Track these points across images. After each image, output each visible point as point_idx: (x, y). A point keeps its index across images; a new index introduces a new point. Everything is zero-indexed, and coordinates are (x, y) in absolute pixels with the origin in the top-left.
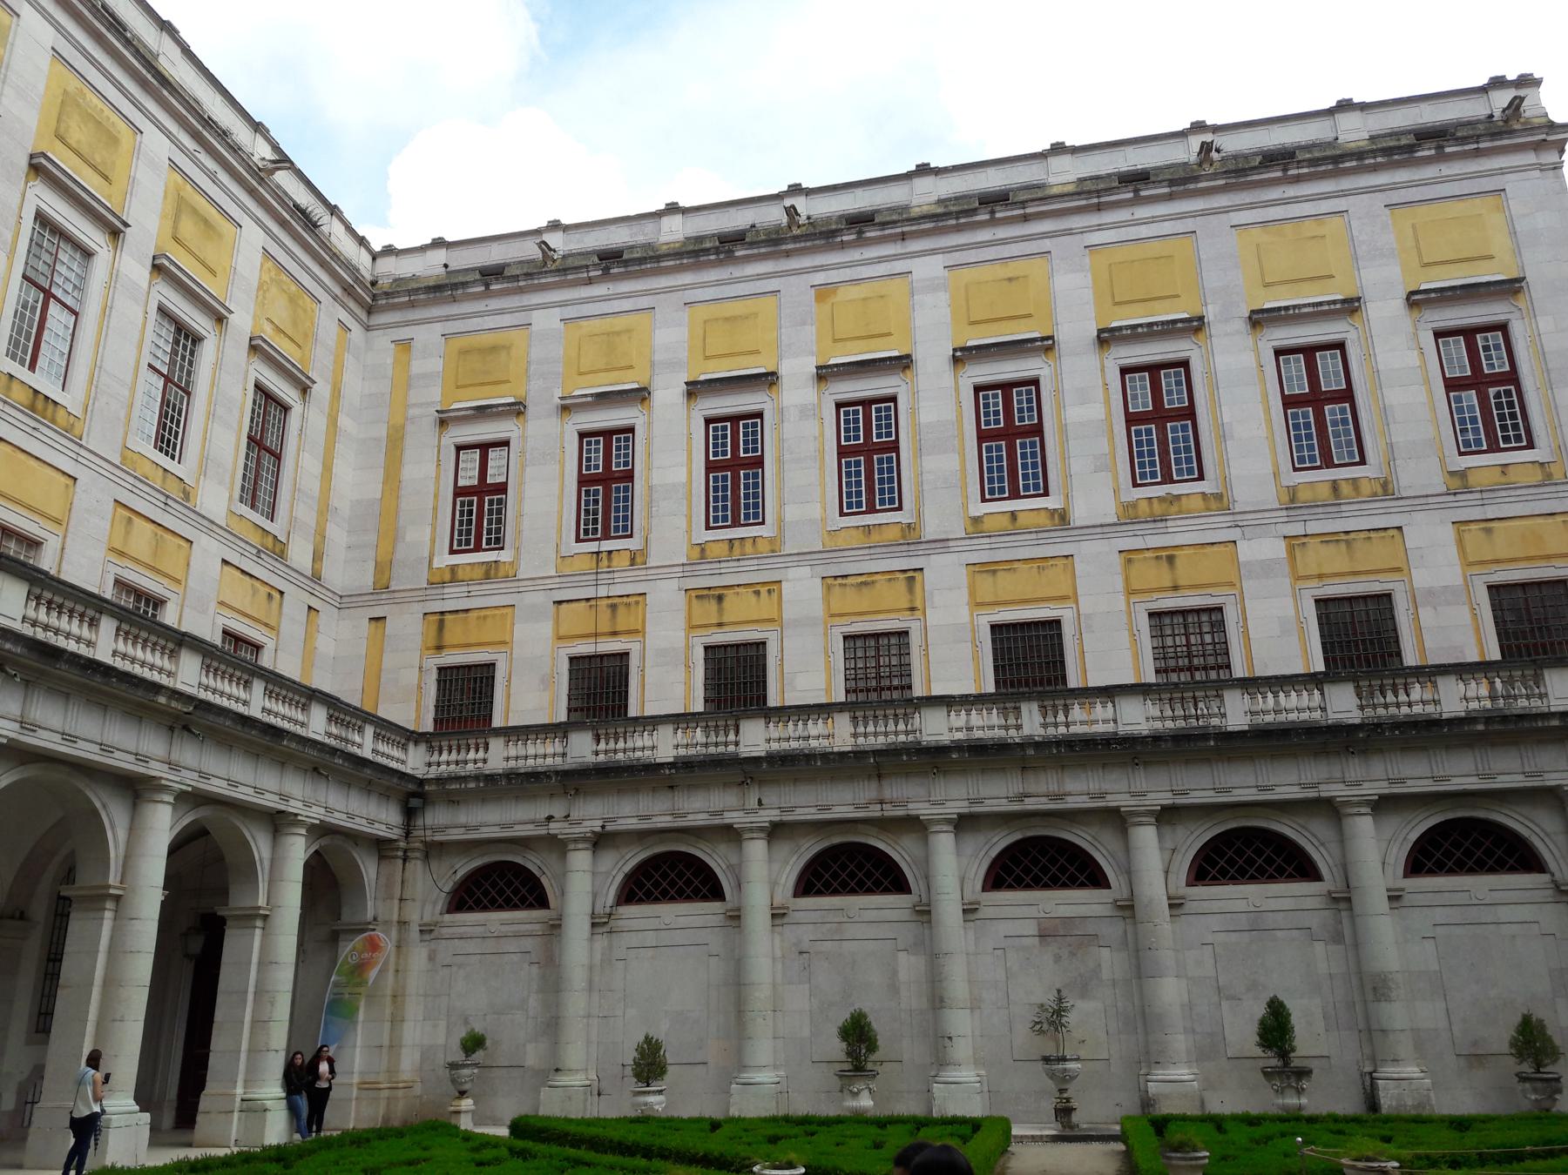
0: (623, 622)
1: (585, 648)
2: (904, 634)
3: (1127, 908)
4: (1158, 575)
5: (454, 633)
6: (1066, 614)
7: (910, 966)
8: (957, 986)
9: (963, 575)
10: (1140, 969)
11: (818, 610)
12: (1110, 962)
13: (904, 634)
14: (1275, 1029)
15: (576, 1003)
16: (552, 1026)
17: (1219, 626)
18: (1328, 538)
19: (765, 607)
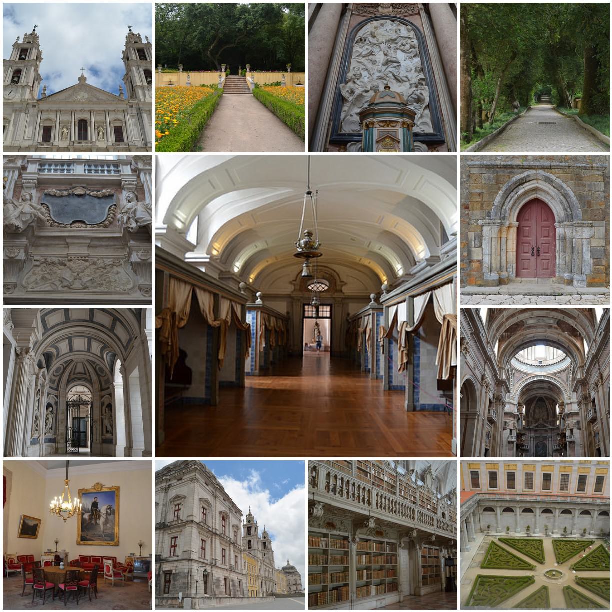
0: (496, 467)
1: (490, 470)
2: (532, 473)
3: (554, 516)
4: (563, 470)
5: (471, 466)
6: (552, 473)
7: (533, 520)
8: (537, 522)
9: (540, 466)
10: (554, 521)
11: (522, 469)
12: (552, 520)
13: (532, 473)
14: (565, 528)
15: (499, 522)
16: (497, 523)
17: (568, 476)
18: (582, 468)
19: (514, 468)
